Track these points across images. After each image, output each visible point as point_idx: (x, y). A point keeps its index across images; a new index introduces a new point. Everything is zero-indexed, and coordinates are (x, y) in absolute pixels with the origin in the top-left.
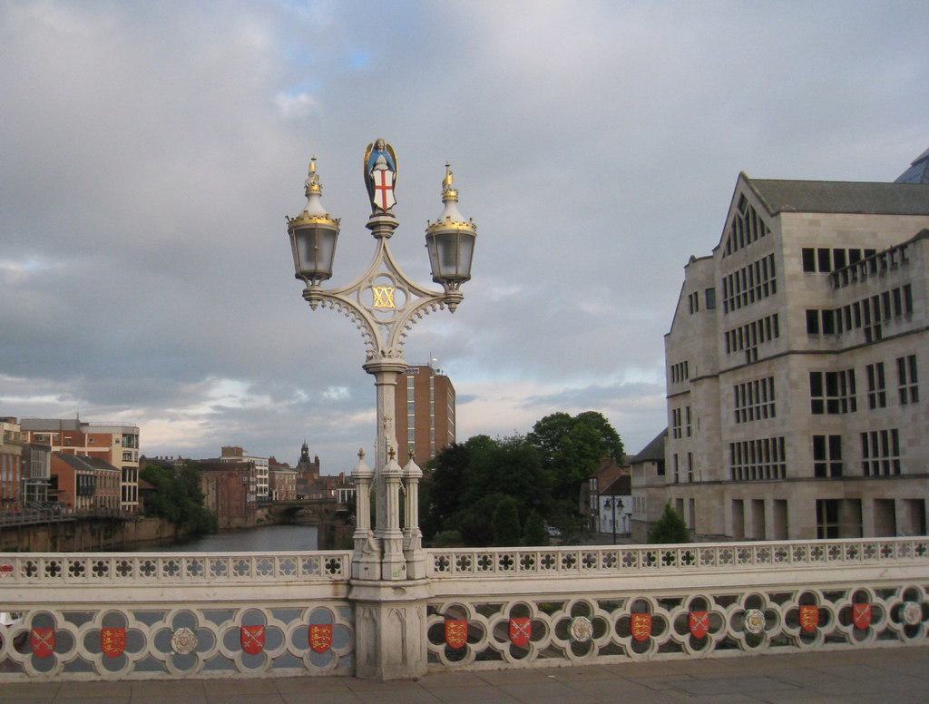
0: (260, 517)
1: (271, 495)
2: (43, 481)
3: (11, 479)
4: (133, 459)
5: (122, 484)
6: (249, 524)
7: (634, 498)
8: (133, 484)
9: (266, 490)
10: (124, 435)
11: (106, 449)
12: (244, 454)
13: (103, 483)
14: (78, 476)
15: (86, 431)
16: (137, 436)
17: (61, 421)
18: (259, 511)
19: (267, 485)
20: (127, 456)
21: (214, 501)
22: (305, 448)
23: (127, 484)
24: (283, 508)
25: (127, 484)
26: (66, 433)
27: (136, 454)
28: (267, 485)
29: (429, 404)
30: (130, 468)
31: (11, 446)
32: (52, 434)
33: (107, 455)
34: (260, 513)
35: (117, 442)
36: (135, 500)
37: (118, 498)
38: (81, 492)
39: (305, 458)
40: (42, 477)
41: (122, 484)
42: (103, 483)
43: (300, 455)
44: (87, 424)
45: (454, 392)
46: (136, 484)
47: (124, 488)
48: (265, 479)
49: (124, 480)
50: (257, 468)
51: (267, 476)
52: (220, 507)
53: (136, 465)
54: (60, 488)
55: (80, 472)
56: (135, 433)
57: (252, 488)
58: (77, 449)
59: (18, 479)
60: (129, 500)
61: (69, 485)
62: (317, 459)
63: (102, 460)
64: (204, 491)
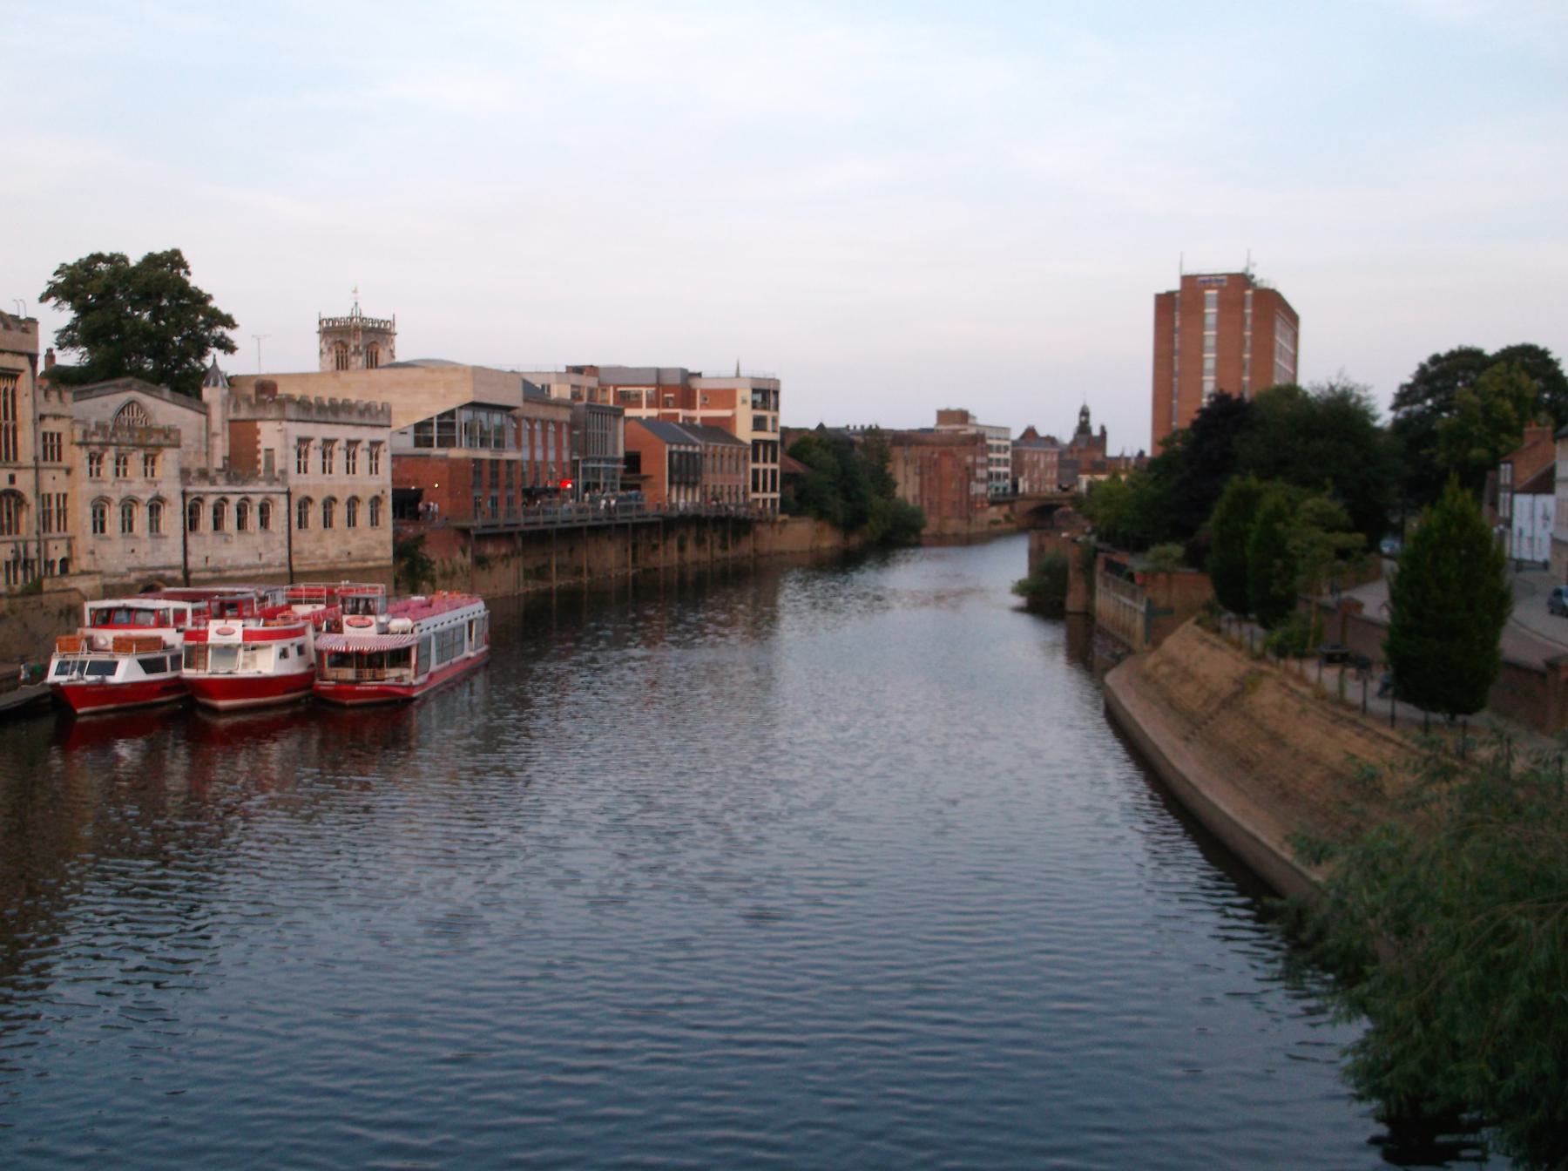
0: (995, 518)
1: (1015, 486)
2: (616, 461)
4: (769, 425)
5: (752, 466)
6: (974, 530)
7: (1558, 500)
8: (770, 466)
9: (1006, 476)
10: (755, 391)
11: (727, 413)
12: (971, 421)
13: (718, 464)
14: (671, 453)
15: (698, 385)
16: (776, 393)
17: (658, 371)
18: (994, 509)
20: (759, 424)
22: (1085, 413)
23: (761, 466)
24: (1030, 505)
25: (761, 466)
26: (668, 388)
27: (775, 420)
29: (1243, 340)
30: (766, 443)
32: (644, 390)
33: (730, 421)
35: (744, 402)
36: (774, 490)
37: (745, 487)
38: (676, 478)
39: (1084, 428)
40: (610, 454)
41: (752, 466)
42: (718, 464)
44: (699, 375)
45: (1293, 318)
46: (776, 466)
47: (755, 472)
49: (755, 459)
50: (989, 442)
51: (1008, 455)
53: (776, 437)
54: (644, 472)
55: (675, 448)
56: (772, 387)
57: (981, 473)
58: (682, 413)
59: (566, 457)
60: (765, 490)
61: (657, 466)
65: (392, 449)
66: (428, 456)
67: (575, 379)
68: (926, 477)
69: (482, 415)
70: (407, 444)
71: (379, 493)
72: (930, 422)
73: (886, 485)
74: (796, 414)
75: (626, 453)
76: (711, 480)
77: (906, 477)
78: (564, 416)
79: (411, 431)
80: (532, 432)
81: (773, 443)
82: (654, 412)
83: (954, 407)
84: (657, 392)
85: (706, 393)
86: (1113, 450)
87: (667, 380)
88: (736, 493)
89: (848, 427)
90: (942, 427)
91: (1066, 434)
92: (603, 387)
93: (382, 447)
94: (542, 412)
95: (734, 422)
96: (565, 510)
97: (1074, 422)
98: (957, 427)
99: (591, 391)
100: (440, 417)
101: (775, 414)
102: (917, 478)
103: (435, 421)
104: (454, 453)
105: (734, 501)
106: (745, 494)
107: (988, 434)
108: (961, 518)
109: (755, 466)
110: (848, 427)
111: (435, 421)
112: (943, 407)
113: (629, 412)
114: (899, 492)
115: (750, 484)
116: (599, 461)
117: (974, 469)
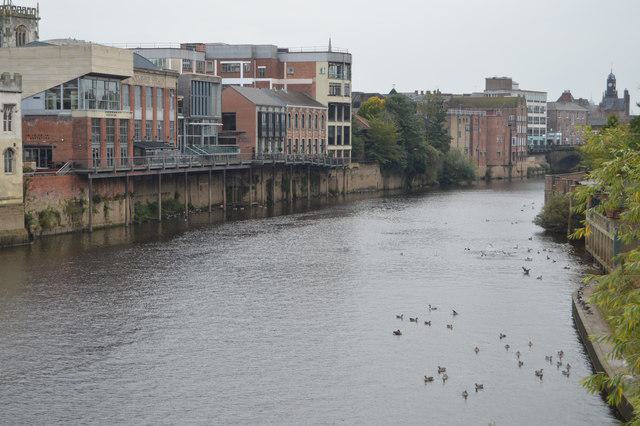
3: (160, 116)
4: (343, 93)
5: (329, 124)
10: (331, 64)
11: (309, 81)
12: (514, 87)
14: (260, 114)
15: (285, 58)
16: (349, 64)
17: (254, 48)
18: (532, 159)
19: (545, 126)
20: (336, 90)
21: (468, 146)
22: (611, 80)
23: (336, 124)
24: (565, 154)
25: (336, 124)
26: (259, 61)
27: (348, 87)
28: (545, 126)
30: (340, 105)
31: (159, 78)
32: (242, 63)
33: (311, 88)
34: (532, 162)
38: (264, 134)
39: (611, 92)
43: (605, 89)
44: (286, 51)
48: (544, 118)
49: (331, 117)
51: (545, 115)
52: (475, 153)
53: (348, 100)
54: (238, 130)
57: (520, 129)
58: (272, 81)
59: (172, 117)
60: (339, 143)
61: (247, 125)
62: (626, 92)
63: (305, 94)
64: (453, 133)
65: (23, 111)
66: (55, 116)
67: (186, 54)
68: (475, 132)
69: (100, 83)
70: (39, 107)
71: (12, 146)
72: (480, 88)
73: (441, 139)
74: (367, 80)
75: (223, 114)
76: (293, 134)
77: (459, 134)
78: (171, 83)
79: (42, 95)
80: (142, 95)
81: (346, 106)
82: (250, 81)
83: (500, 76)
84: (252, 65)
85: (291, 64)
87: (261, 55)
88: (316, 146)
89: (417, 92)
91: (596, 98)
92: (209, 60)
93: (14, 110)
94: (150, 81)
96: (172, 159)
98: (503, 92)
99: (199, 63)
100: (65, 85)
101: (348, 82)
102: (468, 134)
103: (62, 88)
104: (76, 114)
105: (314, 152)
106: (323, 146)
107: (528, 97)
108: (505, 166)
109: (332, 124)
110: (417, 92)
111: (62, 88)
112: (491, 76)
113: (225, 81)
114: (453, 144)
115: (327, 139)
116: (201, 120)
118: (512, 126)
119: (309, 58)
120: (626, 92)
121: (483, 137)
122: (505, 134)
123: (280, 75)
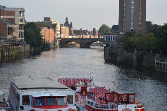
5: (19, 31)
11: (13, 17)
22: (67, 19)
30: (22, 25)
36: (23, 37)
39: (67, 22)
41: (19, 31)
44: (5, 7)
47: (20, 32)
48: (59, 30)
49: (20, 29)
60: (21, 37)
62: (71, 23)
72: (42, 20)
85: (7, 12)
86: (74, 28)
90: (45, 22)
95: (15, 19)
97: (65, 21)
106: (18, 38)
117: (55, 32)
118: (55, 32)
119: (13, 10)
120: (71, 23)
121: (48, 36)
122: (53, 35)
123: (3, 15)
